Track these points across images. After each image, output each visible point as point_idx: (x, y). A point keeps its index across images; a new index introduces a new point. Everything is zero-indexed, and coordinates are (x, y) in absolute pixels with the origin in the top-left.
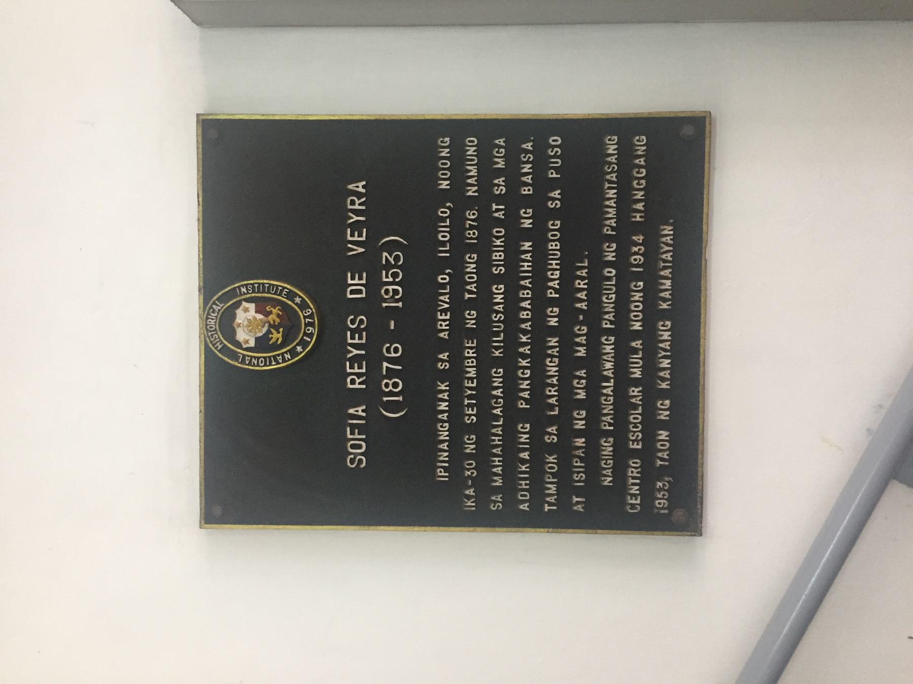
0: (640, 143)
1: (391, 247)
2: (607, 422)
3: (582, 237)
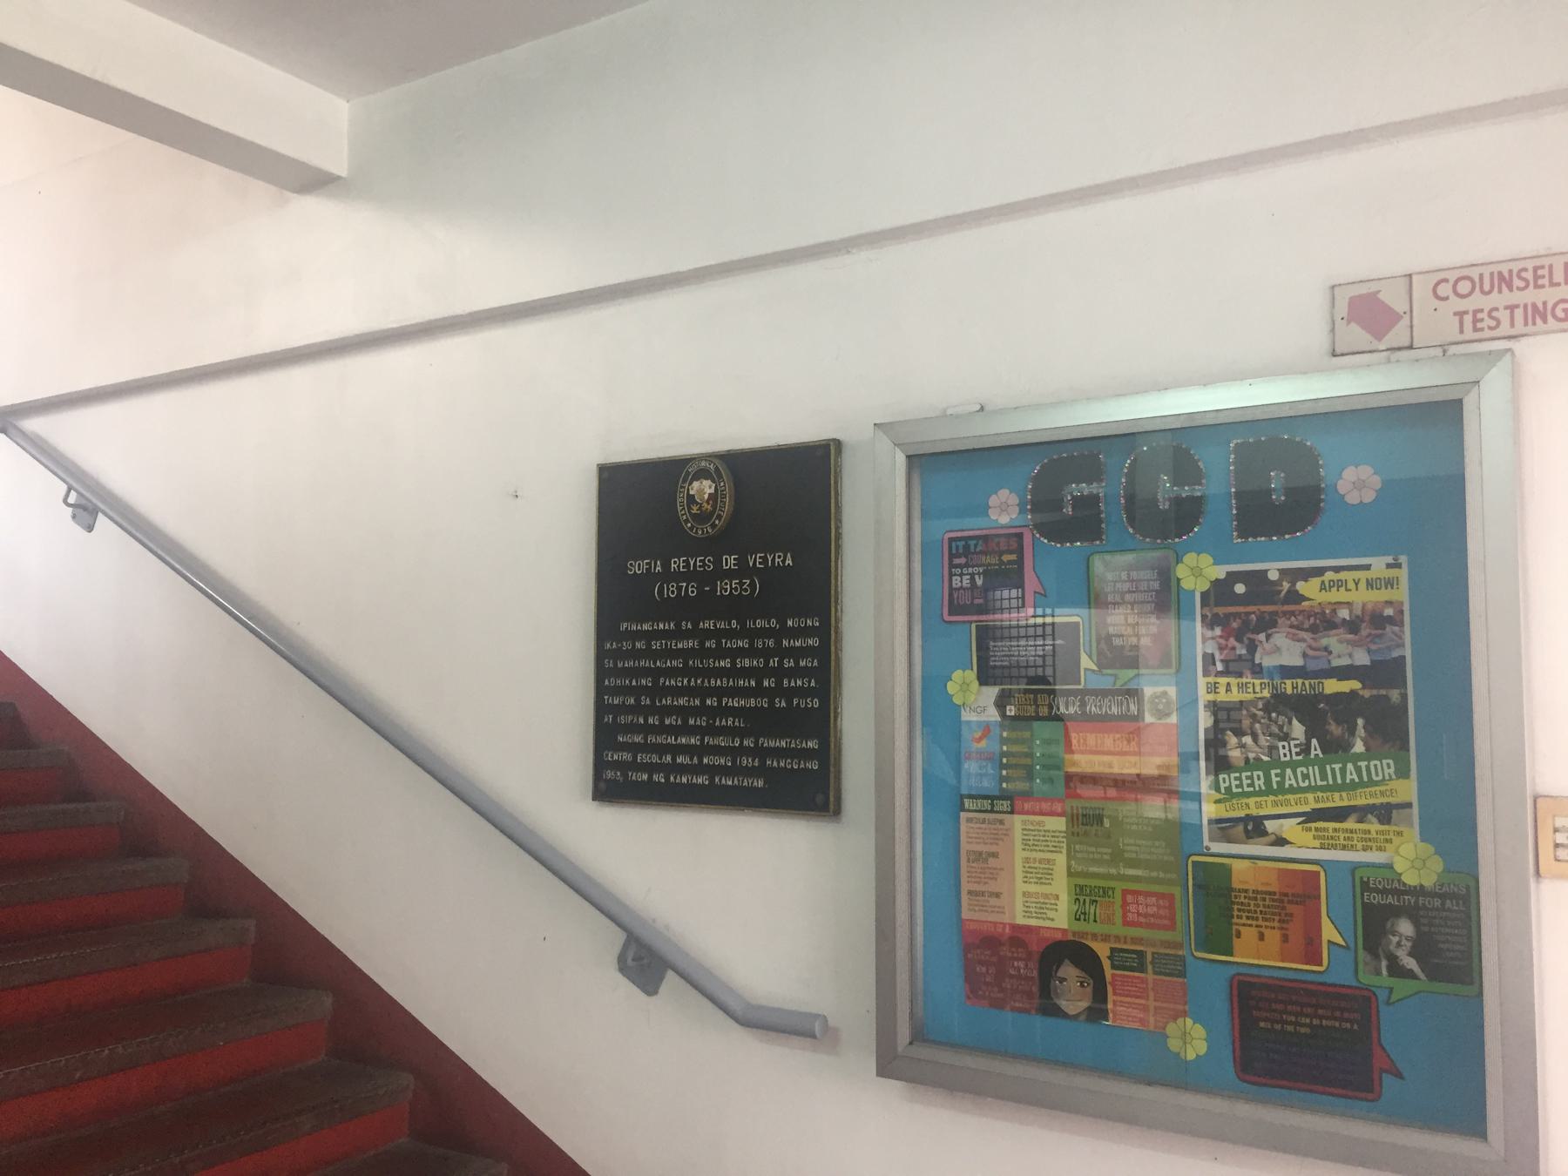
0: (814, 765)
1: (752, 585)
2: (651, 739)
3: (758, 722)
